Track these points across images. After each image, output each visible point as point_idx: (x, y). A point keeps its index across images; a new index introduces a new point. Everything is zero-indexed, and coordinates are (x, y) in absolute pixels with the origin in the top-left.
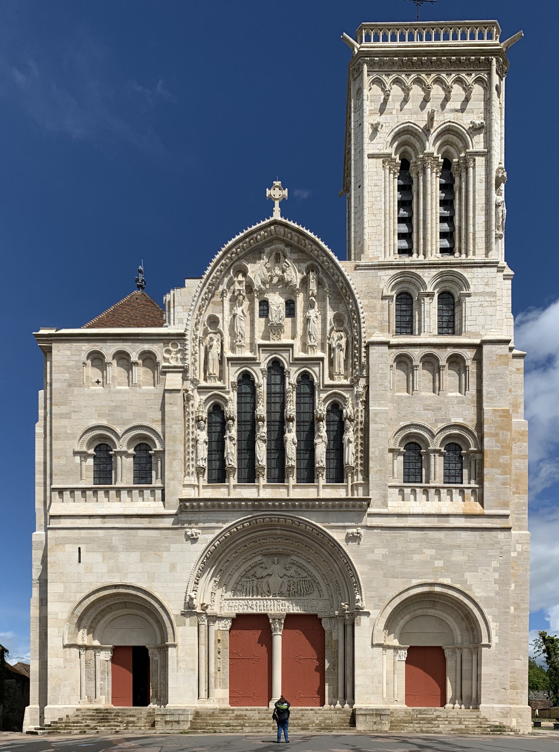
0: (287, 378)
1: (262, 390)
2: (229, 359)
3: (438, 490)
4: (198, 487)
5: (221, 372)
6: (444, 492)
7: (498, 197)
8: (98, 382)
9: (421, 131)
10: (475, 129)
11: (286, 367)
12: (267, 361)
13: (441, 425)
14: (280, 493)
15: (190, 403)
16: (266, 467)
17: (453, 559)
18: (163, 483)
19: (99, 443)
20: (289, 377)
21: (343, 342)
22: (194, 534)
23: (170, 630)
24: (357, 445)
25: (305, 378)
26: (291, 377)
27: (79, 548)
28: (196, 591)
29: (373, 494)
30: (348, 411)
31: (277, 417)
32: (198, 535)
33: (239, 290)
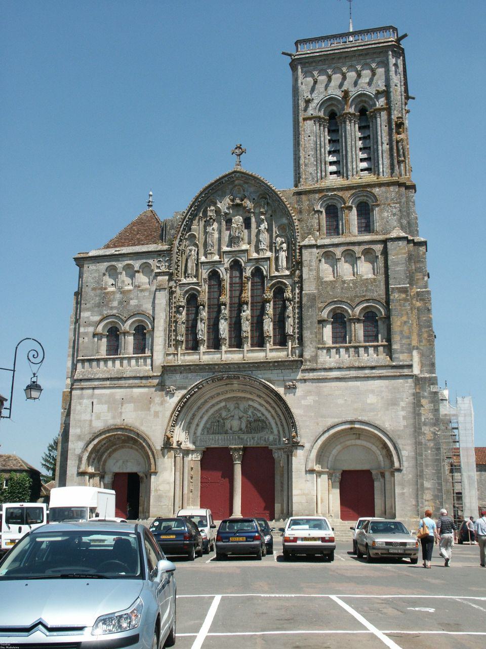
0: (244, 273)
1: (226, 284)
2: (202, 263)
3: (356, 348)
4: (177, 354)
5: (197, 270)
6: (361, 350)
7: (398, 136)
8: (113, 285)
9: (340, 99)
10: (378, 94)
11: (243, 265)
12: (229, 262)
13: (357, 300)
14: (235, 357)
15: (174, 295)
16: (227, 338)
17: (369, 401)
18: (152, 353)
19: (111, 326)
20: (245, 272)
21: (284, 246)
22: (172, 390)
23: (152, 461)
24: (294, 318)
25: (257, 272)
26: (247, 272)
27: (93, 403)
28: (173, 432)
29: (307, 355)
30: (288, 294)
31: (236, 300)
32: (175, 391)
33: (211, 216)
